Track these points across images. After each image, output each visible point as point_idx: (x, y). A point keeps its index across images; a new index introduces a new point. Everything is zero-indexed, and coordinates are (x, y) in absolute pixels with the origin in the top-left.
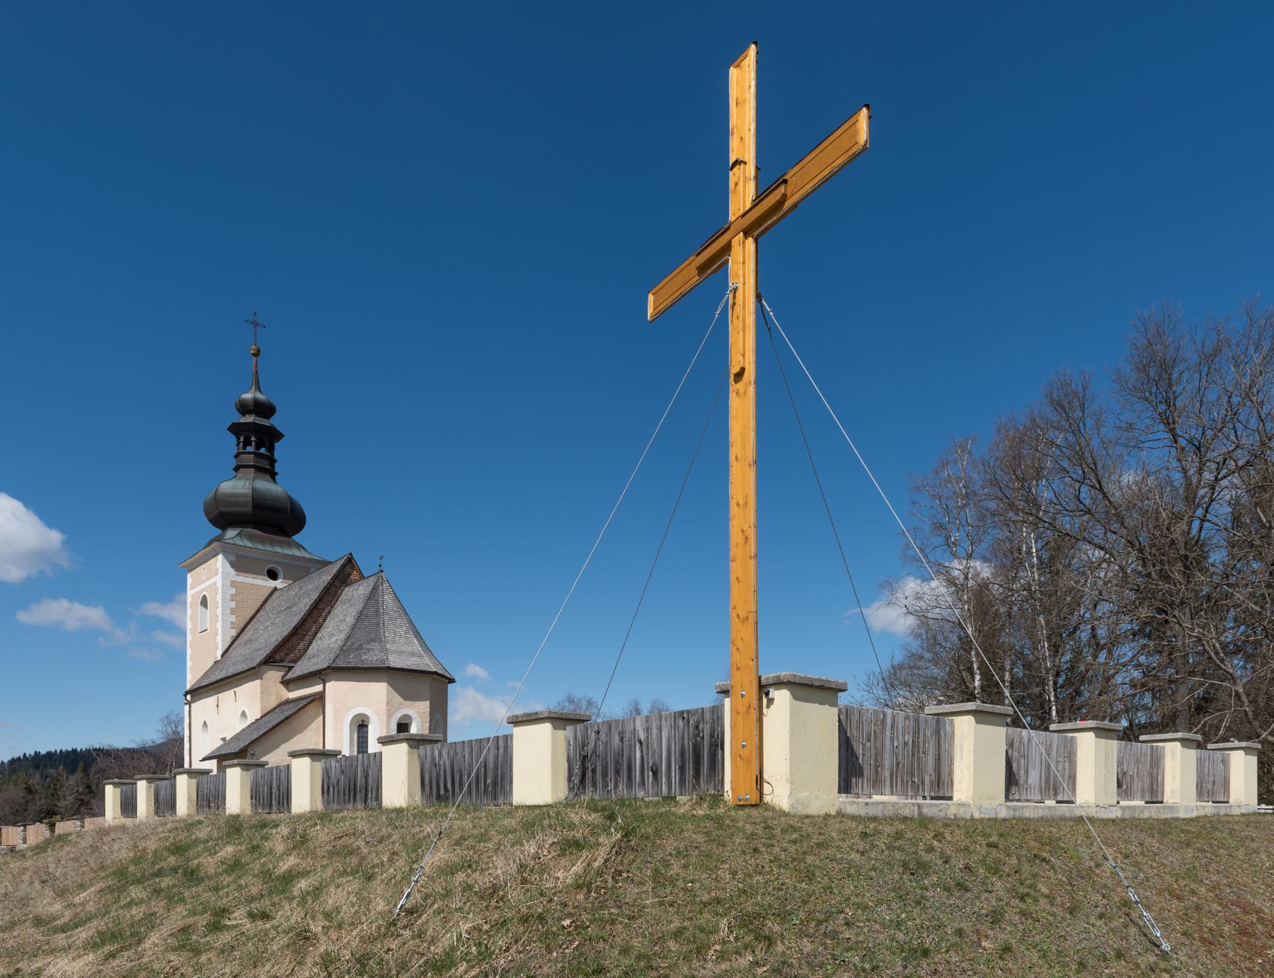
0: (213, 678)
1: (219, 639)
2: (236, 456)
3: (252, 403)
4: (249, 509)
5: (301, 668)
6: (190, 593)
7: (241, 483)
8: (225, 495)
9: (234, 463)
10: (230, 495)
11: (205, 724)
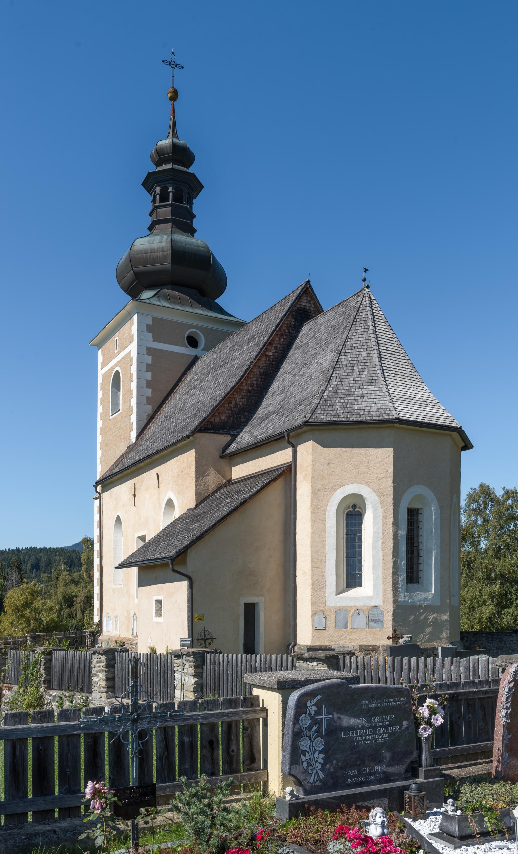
0: (128, 462)
1: (134, 418)
2: (151, 215)
3: (170, 150)
4: (167, 265)
5: (245, 438)
6: (101, 373)
7: (158, 238)
8: (140, 252)
9: (149, 221)
10: (146, 252)
11: (118, 520)
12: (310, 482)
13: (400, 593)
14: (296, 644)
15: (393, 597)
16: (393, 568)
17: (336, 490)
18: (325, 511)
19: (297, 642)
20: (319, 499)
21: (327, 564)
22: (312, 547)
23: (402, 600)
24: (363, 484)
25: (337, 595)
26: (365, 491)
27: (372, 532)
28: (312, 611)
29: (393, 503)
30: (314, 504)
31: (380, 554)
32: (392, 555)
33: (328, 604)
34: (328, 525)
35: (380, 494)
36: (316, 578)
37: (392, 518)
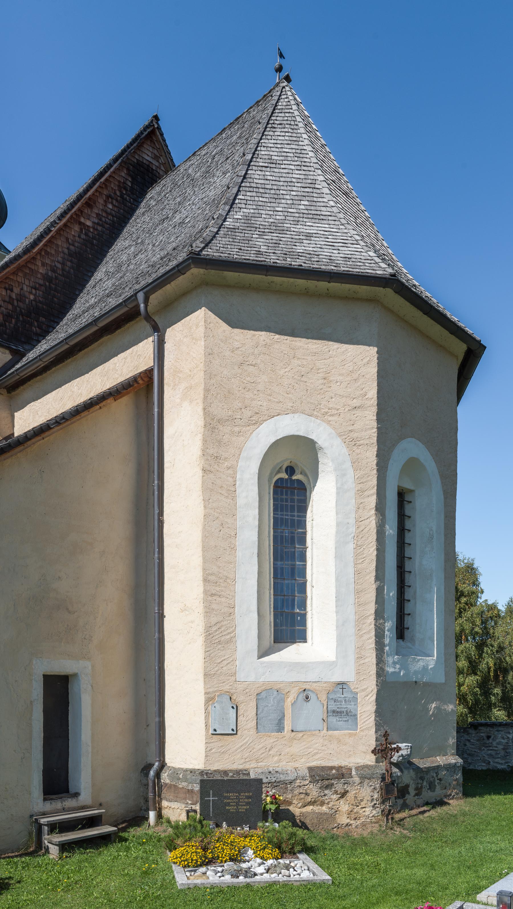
12: (200, 401)
13: (388, 655)
14: (163, 765)
15: (377, 664)
16: (376, 603)
17: (258, 423)
18: (233, 468)
19: (167, 760)
20: (220, 442)
21: (238, 587)
22: (205, 549)
23: (390, 670)
24: (317, 417)
25: (260, 657)
26: (320, 433)
27: (334, 523)
28: (206, 693)
29: (378, 464)
30: (211, 451)
31: (351, 570)
32: (374, 574)
33: (241, 676)
34: (241, 501)
35: (352, 443)
36: (214, 620)
37: (375, 497)
